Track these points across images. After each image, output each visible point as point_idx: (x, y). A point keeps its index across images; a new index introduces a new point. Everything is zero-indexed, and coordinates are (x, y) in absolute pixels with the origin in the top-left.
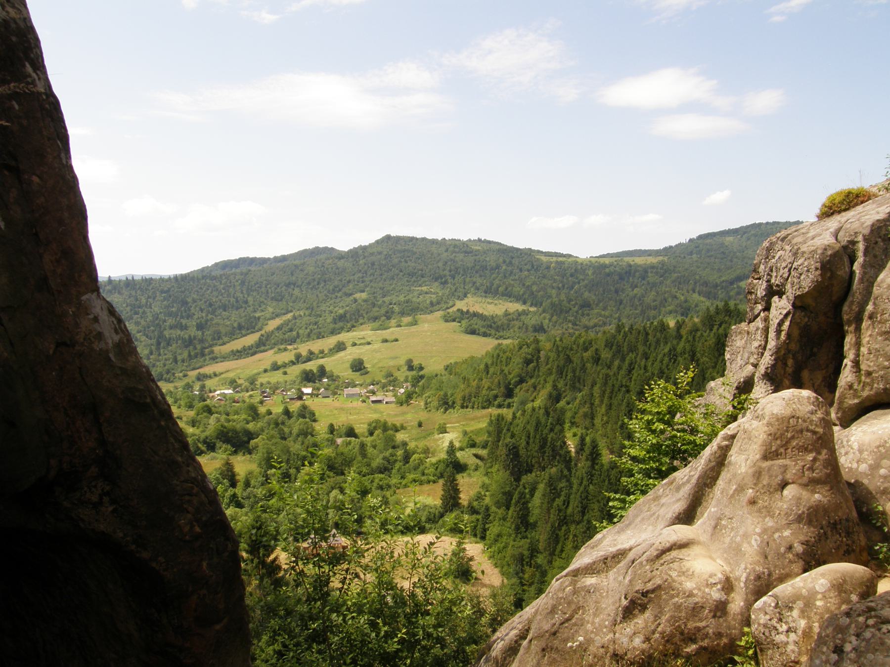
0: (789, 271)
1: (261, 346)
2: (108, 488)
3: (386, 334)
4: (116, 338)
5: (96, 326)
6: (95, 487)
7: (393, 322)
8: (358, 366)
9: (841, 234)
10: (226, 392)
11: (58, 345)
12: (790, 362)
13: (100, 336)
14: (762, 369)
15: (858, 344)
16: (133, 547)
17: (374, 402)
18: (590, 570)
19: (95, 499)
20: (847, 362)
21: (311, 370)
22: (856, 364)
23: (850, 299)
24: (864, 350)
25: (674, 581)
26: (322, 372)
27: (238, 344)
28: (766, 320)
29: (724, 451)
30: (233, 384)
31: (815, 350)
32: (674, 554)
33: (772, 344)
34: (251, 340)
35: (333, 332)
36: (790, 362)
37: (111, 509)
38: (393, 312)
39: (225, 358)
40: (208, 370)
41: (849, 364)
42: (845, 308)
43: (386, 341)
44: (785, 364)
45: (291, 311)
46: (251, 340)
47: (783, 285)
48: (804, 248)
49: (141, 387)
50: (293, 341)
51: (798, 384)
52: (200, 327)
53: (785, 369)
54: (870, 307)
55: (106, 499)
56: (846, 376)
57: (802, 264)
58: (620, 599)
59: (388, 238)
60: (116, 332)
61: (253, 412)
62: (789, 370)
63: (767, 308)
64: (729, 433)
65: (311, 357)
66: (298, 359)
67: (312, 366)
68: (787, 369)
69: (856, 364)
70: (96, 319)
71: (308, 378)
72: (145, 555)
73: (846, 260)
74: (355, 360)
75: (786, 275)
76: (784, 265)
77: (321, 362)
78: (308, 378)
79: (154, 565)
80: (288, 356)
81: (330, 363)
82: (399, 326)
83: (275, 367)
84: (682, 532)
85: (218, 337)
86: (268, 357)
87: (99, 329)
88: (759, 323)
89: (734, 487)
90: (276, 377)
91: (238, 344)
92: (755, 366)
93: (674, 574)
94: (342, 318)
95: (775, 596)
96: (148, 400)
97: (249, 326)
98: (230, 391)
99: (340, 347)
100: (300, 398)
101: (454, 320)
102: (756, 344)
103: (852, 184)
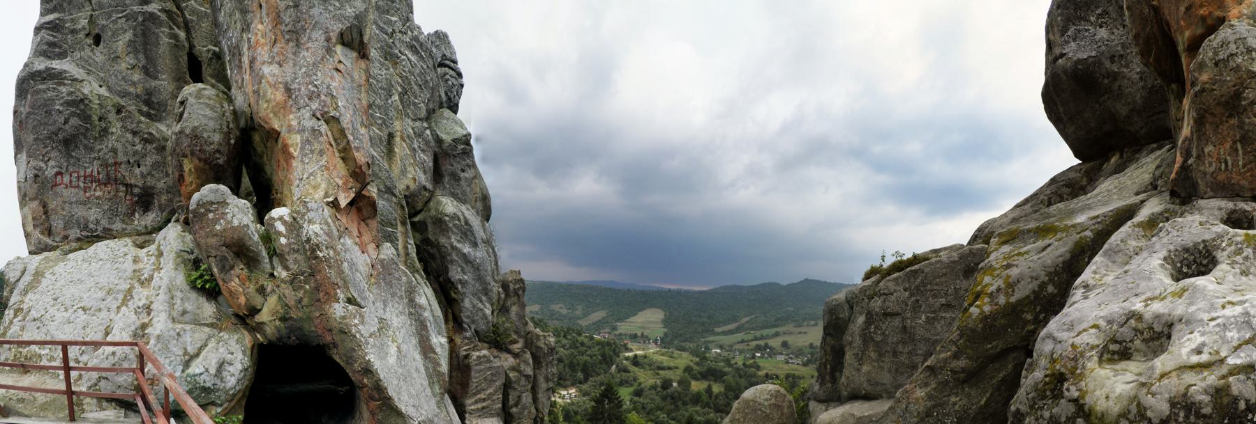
1: (737, 330)
8: (785, 344)
26: (766, 346)
27: (726, 328)
30: (721, 347)
34: (732, 326)
39: (718, 334)
40: (711, 338)
46: (732, 326)
50: (753, 329)
52: (709, 317)
61: (727, 361)
66: (756, 339)
67: (762, 343)
71: (758, 348)
78: (758, 348)
80: (750, 337)
81: (772, 343)
83: (743, 341)
85: (719, 324)
86: (740, 336)
90: (740, 346)
91: (726, 328)
94: (778, 319)
97: (735, 320)
99: (777, 334)
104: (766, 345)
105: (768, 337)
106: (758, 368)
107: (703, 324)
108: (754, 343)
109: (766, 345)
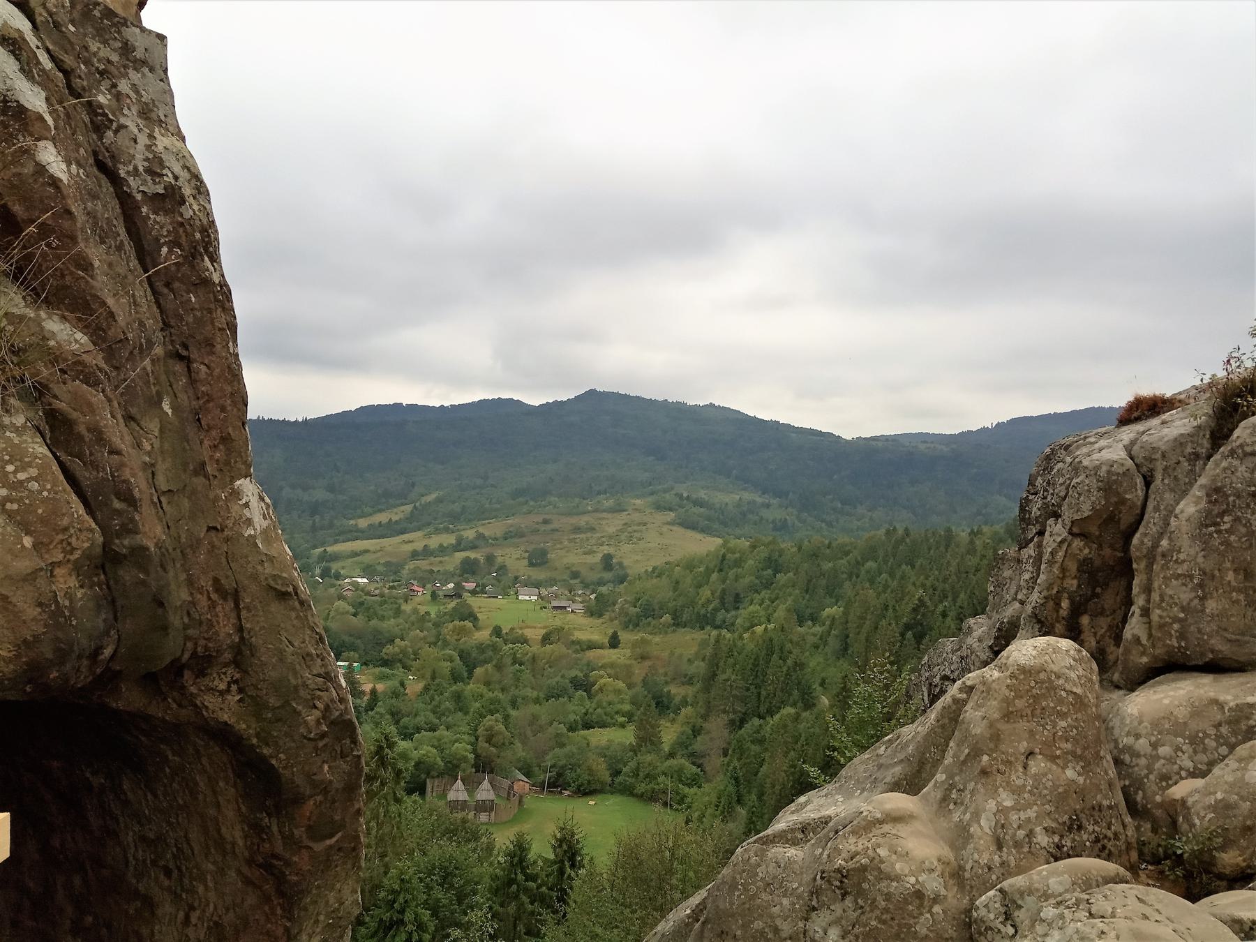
0: (1067, 488)
2: (237, 676)
4: (265, 524)
5: (246, 511)
6: (225, 673)
9: (1136, 448)
10: (360, 580)
11: (210, 529)
12: (1065, 604)
13: (249, 522)
14: (1029, 609)
15: (1148, 590)
16: (255, 741)
18: (784, 838)
19: (222, 686)
20: (1135, 608)
22: (1146, 612)
23: (1141, 529)
24: (1155, 597)
25: (882, 862)
27: (382, 518)
28: (1039, 545)
29: (959, 704)
30: (368, 571)
31: (1098, 590)
32: (886, 828)
33: (1042, 577)
36: (1065, 604)
37: (238, 698)
41: (1138, 611)
42: (1135, 541)
43: (577, 530)
45: (456, 480)
47: (1060, 506)
48: (1086, 463)
49: (284, 575)
51: (1073, 633)
54: (1164, 543)
55: (234, 687)
56: (1134, 627)
57: (1082, 482)
58: (815, 879)
59: (592, 393)
60: (265, 518)
62: (1064, 613)
63: (1041, 533)
64: (969, 683)
69: (1146, 612)
70: (247, 505)
72: (266, 751)
73: (1139, 481)
75: (1062, 494)
76: (1061, 480)
78: (469, 568)
79: (274, 762)
80: (448, 539)
82: (596, 511)
83: (427, 552)
84: (899, 801)
86: (417, 540)
87: (248, 515)
88: (1031, 551)
89: (967, 751)
92: (1022, 603)
93: (883, 852)
95: (1001, 890)
96: (291, 589)
98: (365, 580)
100: (459, 596)
101: (671, 510)
102: (1027, 576)
103: (1147, 391)
106: (472, 617)
107: (315, 509)
108: (460, 556)
109: (490, 559)
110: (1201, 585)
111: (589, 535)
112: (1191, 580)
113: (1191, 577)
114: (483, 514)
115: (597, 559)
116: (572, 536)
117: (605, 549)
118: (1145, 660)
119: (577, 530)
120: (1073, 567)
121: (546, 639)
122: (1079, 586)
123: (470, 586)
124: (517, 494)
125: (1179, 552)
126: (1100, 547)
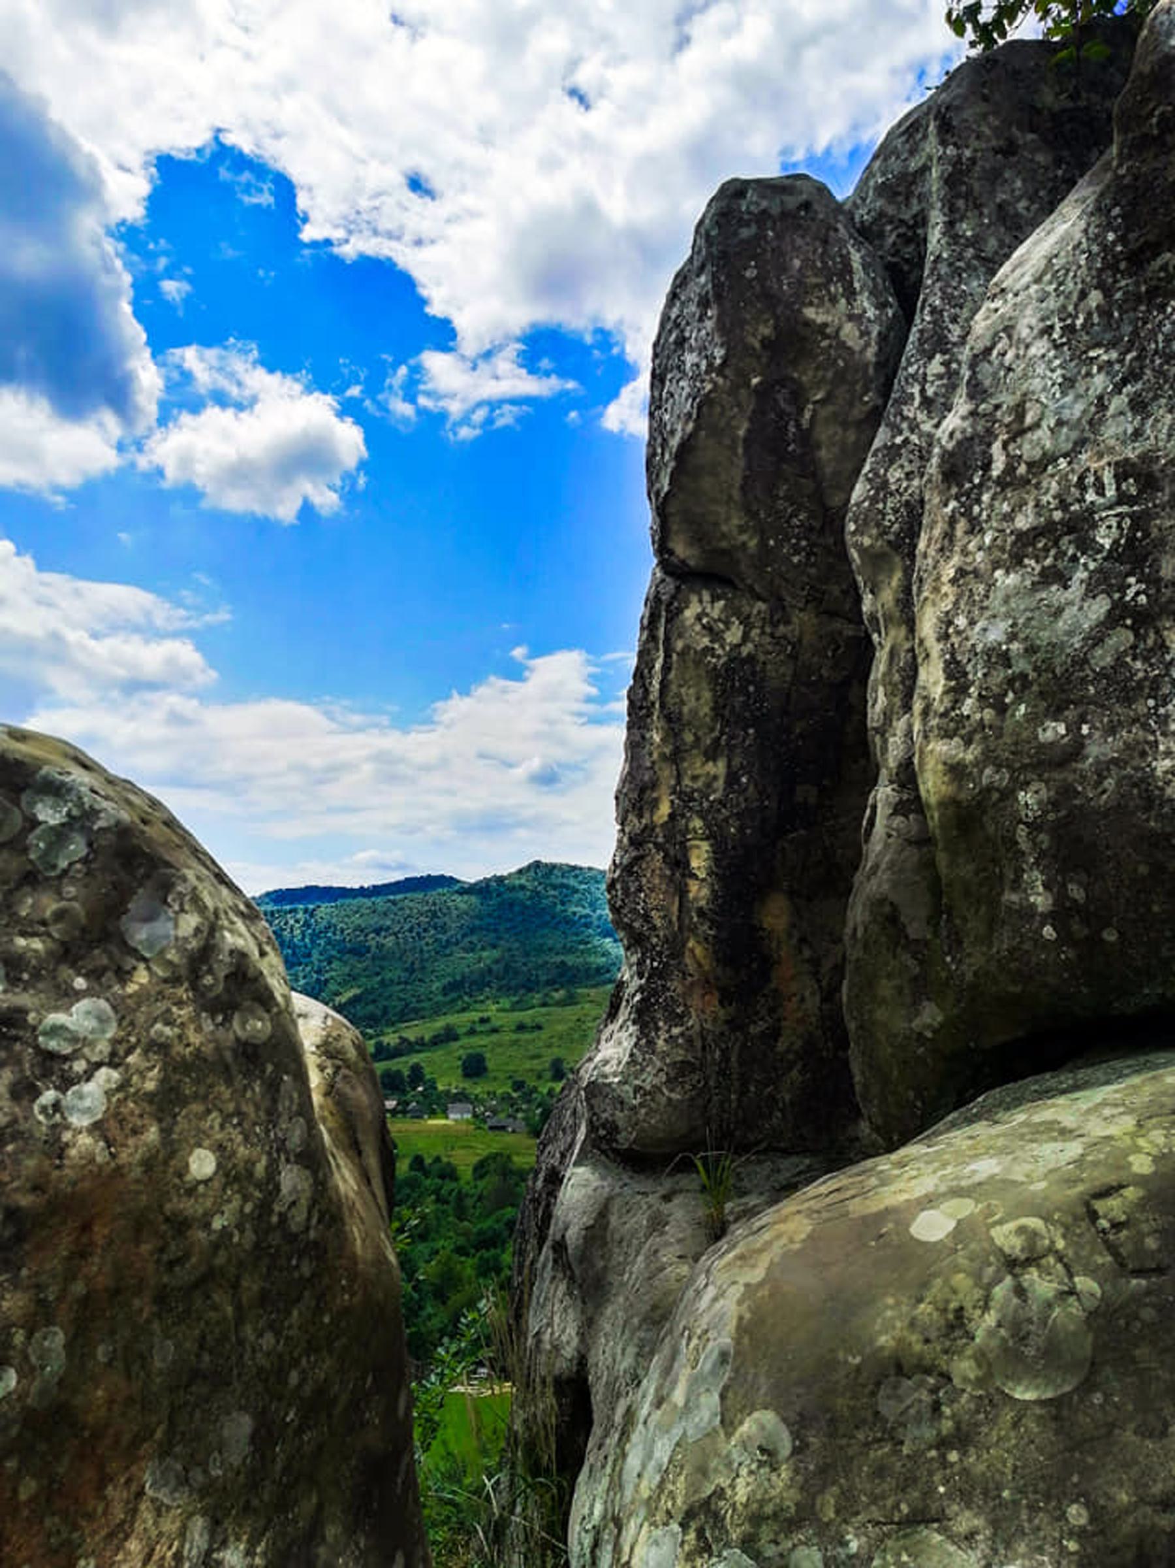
3: (525, 1016)
7: (537, 997)
12: (700, 859)
17: (491, 1128)
21: (399, 1072)
26: (417, 1073)
35: (437, 1011)
36: (700, 859)
38: (538, 983)
43: (521, 1028)
44: (679, 864)
45: (378, 974)
53: (683, 892)
59: (537, 864)
62: (699, 892)
65: (406, 1047)
67: (402, 1065)
68: (694, 887)
74: (470, 1056)
77: (415, 1059)
82: (544, 1005)
99: (449, 1035)
104: (417, 1071)
105: (420, 1045)
109: (417, 1071)
110: (1135, 553)
111: (535, 1034)
112: (1087, 545)
113: (1079, 526)
114: (406, 1014)
115: (545, 1063)
116: (514, 1036)
117: (556, 1052)
118: (930, 1015)
119: (521, 1028)
120: (697, 700)
121: (480, 1169)
122: (732, 778)
123: (390, 1104)
124: (454, 986)
125: (1018, 431)
126: (779, 613)
